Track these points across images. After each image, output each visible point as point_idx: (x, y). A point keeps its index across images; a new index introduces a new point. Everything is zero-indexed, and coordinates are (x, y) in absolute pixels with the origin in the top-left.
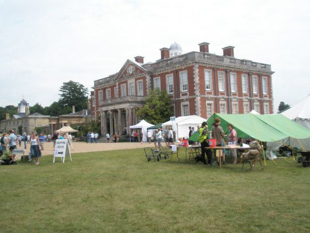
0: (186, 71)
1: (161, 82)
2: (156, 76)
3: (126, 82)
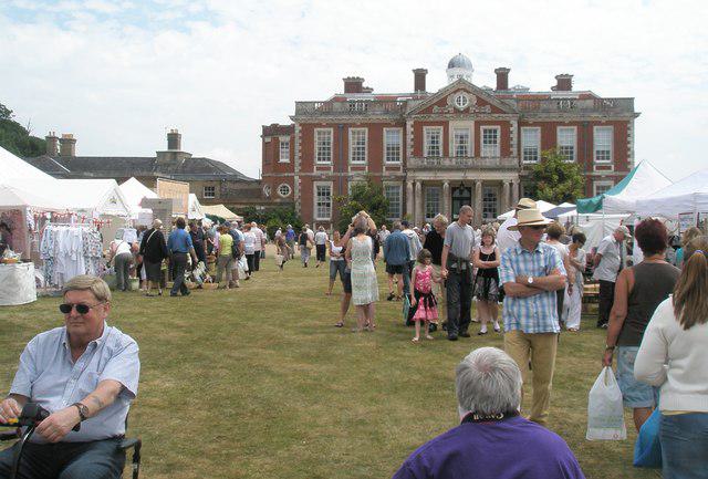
0: (612, 127)
1: (542, 137)
2: (527, 124)
3: (445, 124)
